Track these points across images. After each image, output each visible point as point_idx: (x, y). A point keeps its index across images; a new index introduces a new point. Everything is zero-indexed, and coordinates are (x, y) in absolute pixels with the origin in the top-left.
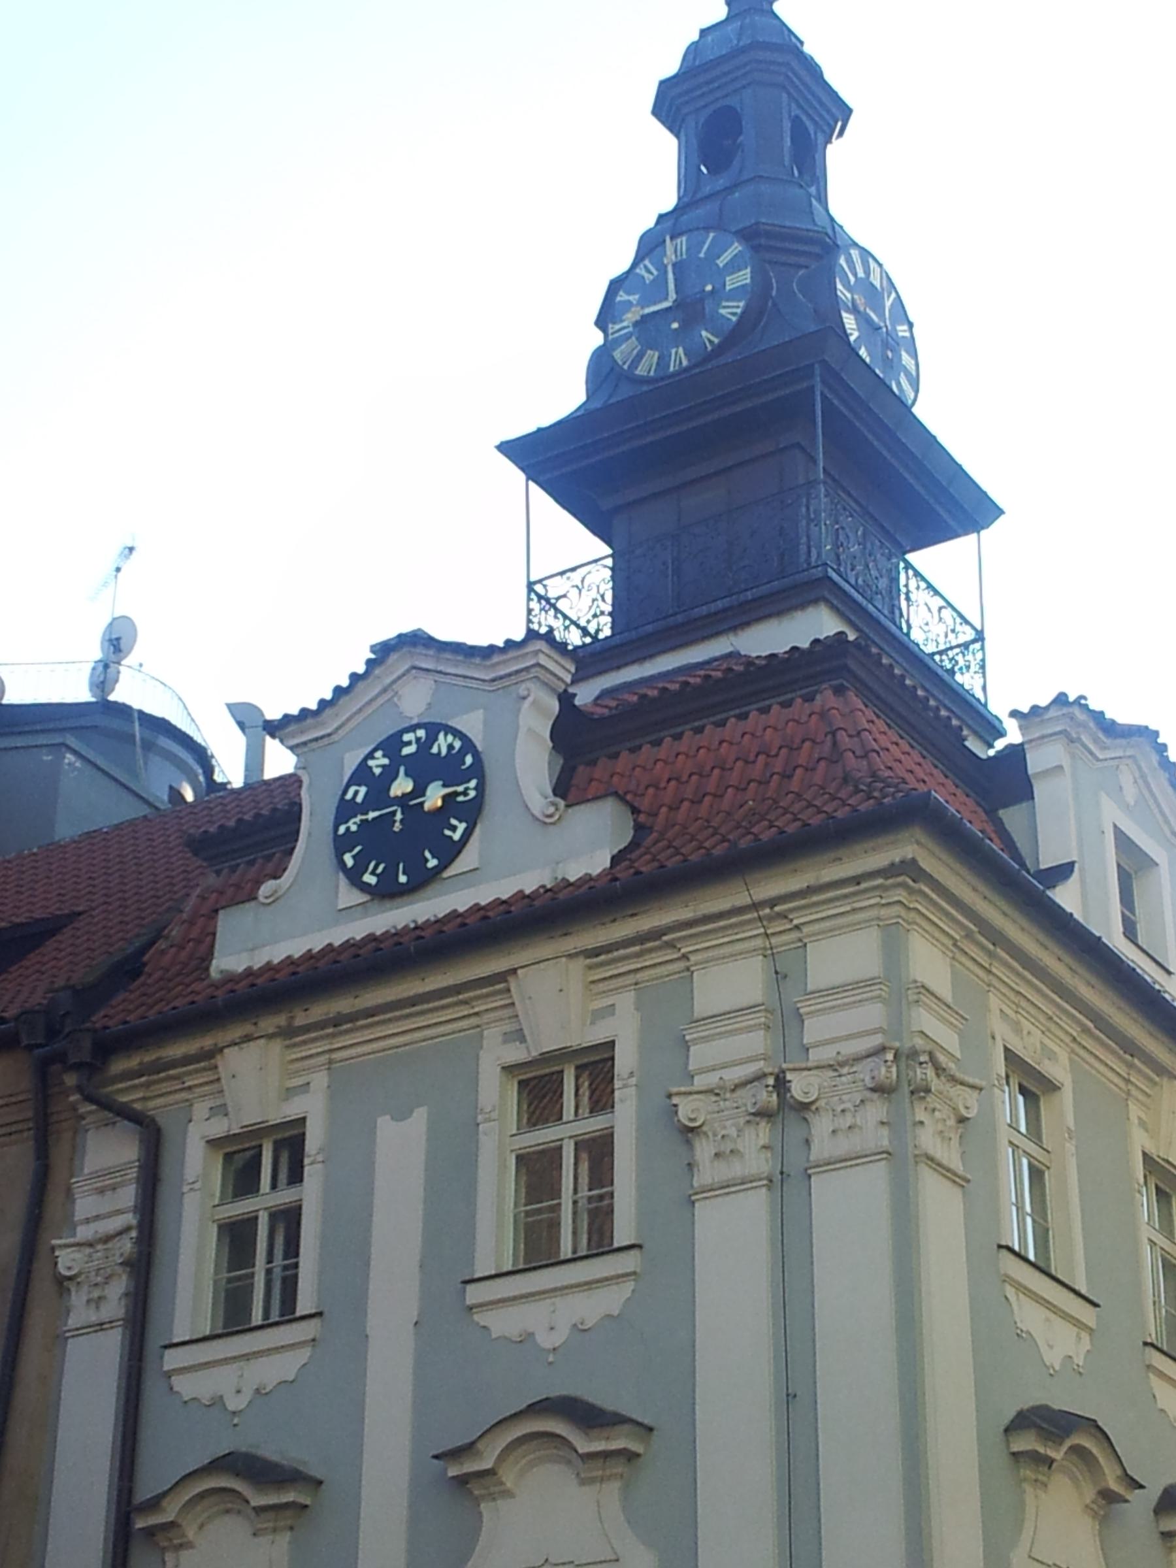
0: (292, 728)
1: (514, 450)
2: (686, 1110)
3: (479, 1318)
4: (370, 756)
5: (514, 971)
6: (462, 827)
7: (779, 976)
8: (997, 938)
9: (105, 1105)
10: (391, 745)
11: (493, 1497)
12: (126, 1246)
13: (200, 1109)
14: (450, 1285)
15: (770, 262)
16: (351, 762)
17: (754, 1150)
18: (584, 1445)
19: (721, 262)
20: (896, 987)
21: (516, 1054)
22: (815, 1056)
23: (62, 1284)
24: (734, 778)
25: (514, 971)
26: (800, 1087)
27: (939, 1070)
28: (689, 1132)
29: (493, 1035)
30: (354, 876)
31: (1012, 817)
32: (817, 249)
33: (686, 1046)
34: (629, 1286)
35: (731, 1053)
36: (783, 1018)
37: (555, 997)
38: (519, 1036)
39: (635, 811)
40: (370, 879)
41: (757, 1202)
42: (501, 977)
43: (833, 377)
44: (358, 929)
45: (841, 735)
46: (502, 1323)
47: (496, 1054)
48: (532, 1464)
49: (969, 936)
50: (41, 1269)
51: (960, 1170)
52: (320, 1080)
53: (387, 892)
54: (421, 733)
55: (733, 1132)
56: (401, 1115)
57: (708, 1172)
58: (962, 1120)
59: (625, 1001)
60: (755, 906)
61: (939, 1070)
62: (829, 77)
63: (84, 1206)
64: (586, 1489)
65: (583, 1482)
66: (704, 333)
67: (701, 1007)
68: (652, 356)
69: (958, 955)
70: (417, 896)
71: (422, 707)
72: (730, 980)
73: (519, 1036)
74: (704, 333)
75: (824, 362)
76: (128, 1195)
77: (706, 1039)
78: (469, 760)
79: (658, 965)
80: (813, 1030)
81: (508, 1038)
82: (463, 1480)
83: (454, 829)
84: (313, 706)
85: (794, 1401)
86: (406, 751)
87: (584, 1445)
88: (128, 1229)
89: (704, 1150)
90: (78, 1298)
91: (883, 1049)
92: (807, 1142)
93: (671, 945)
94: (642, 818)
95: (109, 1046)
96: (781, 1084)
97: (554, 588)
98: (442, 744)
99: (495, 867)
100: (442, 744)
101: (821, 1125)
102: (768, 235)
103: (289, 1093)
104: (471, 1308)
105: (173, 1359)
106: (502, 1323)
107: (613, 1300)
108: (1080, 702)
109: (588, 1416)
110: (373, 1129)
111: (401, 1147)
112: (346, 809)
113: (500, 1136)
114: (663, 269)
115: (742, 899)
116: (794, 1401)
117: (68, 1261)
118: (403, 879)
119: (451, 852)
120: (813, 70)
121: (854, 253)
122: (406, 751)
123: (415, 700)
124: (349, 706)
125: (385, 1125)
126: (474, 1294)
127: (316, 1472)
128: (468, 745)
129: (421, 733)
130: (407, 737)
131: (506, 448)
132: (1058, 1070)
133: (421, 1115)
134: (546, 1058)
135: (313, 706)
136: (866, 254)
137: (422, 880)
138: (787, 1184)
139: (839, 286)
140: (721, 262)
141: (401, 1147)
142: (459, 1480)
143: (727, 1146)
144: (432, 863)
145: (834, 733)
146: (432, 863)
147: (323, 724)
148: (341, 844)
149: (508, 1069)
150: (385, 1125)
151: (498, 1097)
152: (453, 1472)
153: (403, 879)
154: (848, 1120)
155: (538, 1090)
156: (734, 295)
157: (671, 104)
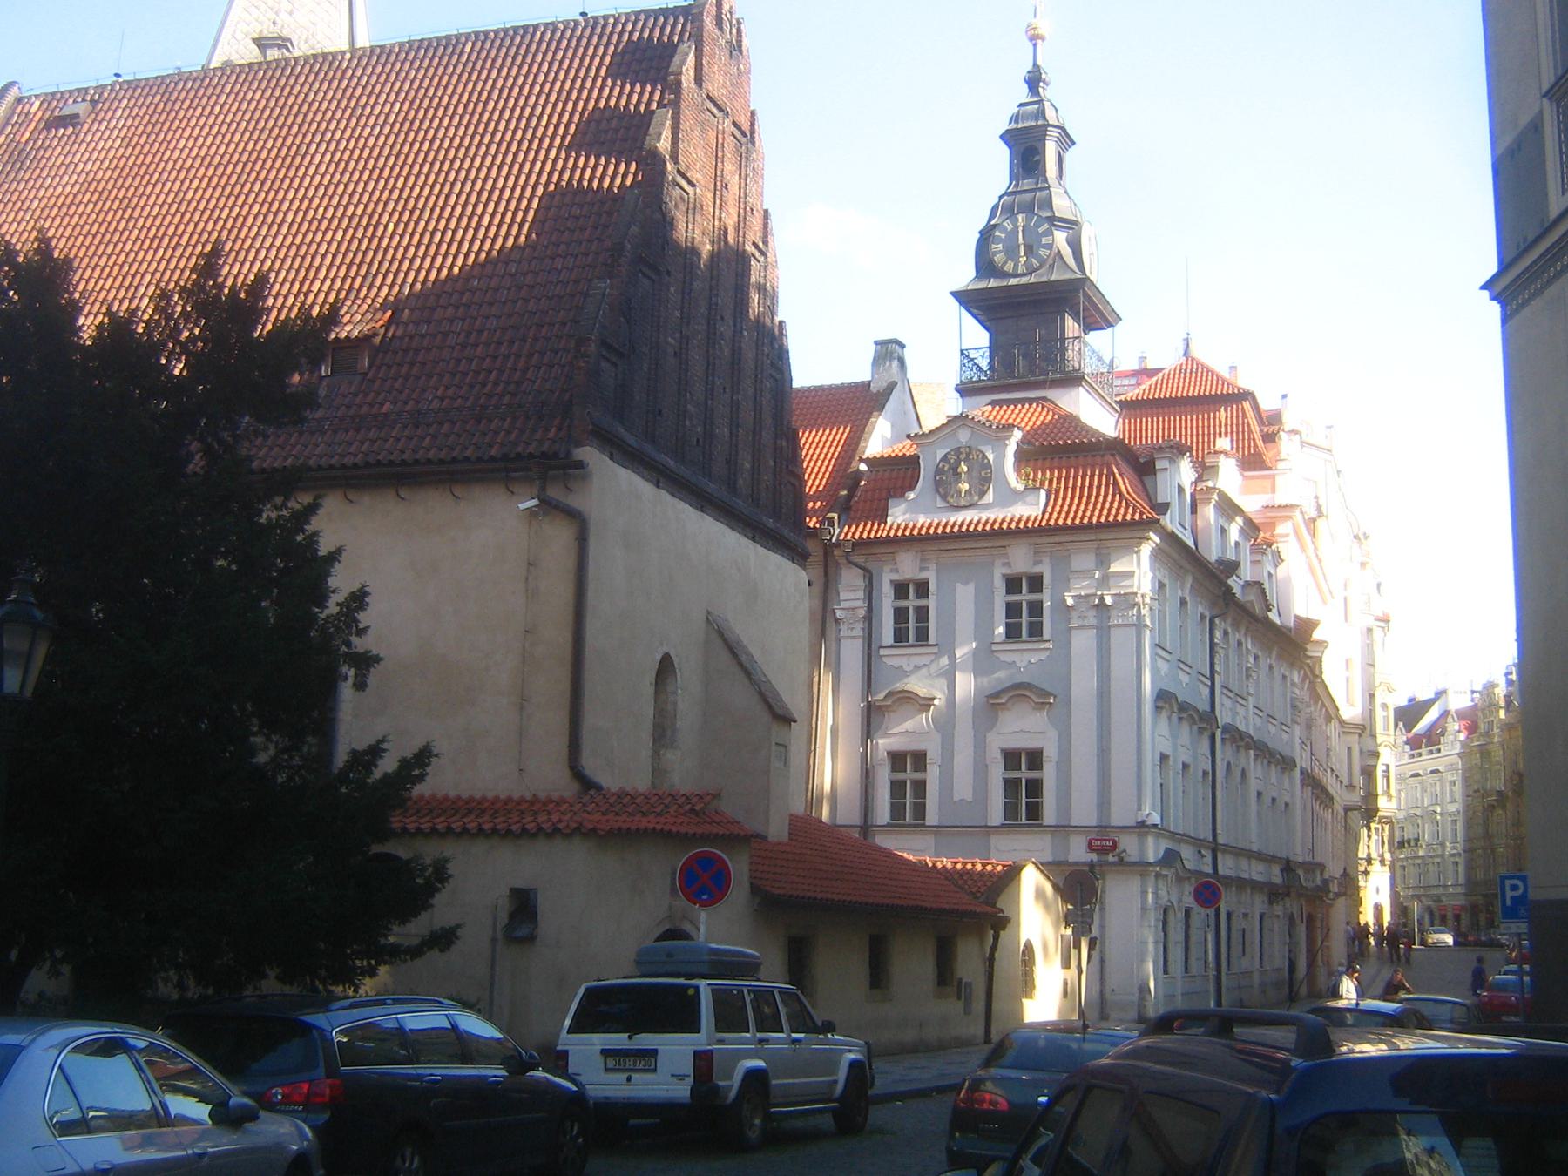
1: (955, 294)
12: (862, 612)
13: (887, 568)
16: (940, 454)
23: (837, 621)
29: (998, 562)
30: (944, 498)
31: (1147, 480)
38: (1008, 565)
43: (1086, 295)
46: (1004, 657)
50: (829, 615)
56: (966, 583)
63: (842, 596)
72: (1083, 560)
73: (1008, 565)
76: (861, 594)
81: (1004, 565)
90: (843, 627)
97: (973, 354)
103: (922, 569)
105: (882, 652)
106: (1004, 657)
111: (965, 595)
112: (938, 471)
113: (1000, 600)
114: (1016, 228)
117: (839, 614)
123: (964, 436)
125: (959, 585)
126: (994, 648)
131: (954, 294)
132: (1166, 581)
133: (971, 587)
141: (965, 595)
150: (960, 588)
157: (1007, 137)
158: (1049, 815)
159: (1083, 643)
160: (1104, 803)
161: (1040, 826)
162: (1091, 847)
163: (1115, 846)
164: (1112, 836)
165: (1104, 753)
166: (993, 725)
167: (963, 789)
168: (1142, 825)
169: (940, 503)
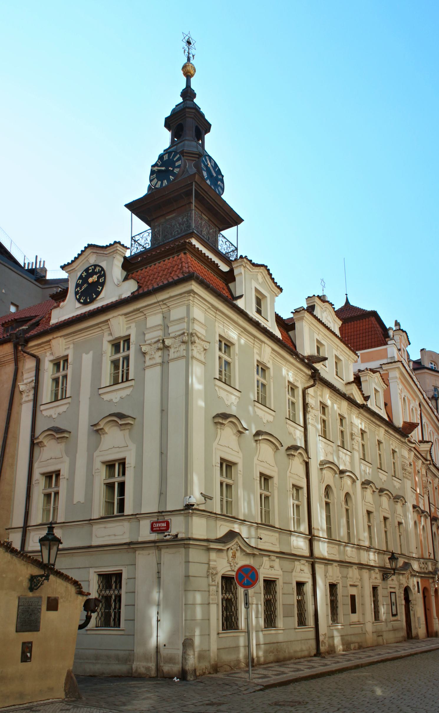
0: (66, 267)
2: (144, 349)
3: (102, 397)
4: (83, 273)
5: (109, 319)
6: (101, 288)
7: (164, 317)
8: (217, 309)
9: (28, 353)
10: (87, 270)
11: (103, 434)
14: (97, 390)
15: (187, 159)
17: (158, 357)
18: (120, 422)
19: (175, 159)
20: (189, 319)
21: (111, 338)
22: (171, 335)
24: (160, 275)
25: (109, 319)
26: (167, 342)
27: (198, 338)
28: (144, 354)
29: (106, 334)
30: (79, 300)
32: (197, 156)
33: (144, 334)
34: (131, 389)
35: (152, 336)
36: (166, 327)
37: (119, 324)
38: (111, 334)
39: (138, 283)
40: (82, 301)
41: (158, 369)
42: (107, 321)
44: (79, 312)
45: (184, 263)
46: (106, 397)
47: (107, 338)
48: (112, 427)
49: (209, 308)
51: (204, 361)
52: (71, 346)
53: (85, 303)
54: (93, 267)
55: (153, 353)
57: (148, 363)
58: (205, 350)
59: (133, 325)
60: (158, 302)
61: (198, 338)
62: (207, 117)
64: (122, 432)
65: (121, 430)
66: (171, 177)
67: (149, 325)
68: (159, 183)
69: (207, 313)
70: (92, 304)
71: (94, 261)
72: (154, 319)
74: (171, 177)
75: (195, 182)
77: (149, 333)
78: (103, 272)
79: (139, 316)
80: (171, 330)
82: (97, 431)
83: (99, 288)
84: (70, 262)
85: (164, 411)
86: (90, 271)
87: (120, 422)
88: (33, 381)
89: (147, 357)
91: (184, 333)
92: (169, 355)
93: (142, 312)
94: (141, 285)
95: (27, 341)
96: (163, 342)
98: (97, 269)
99: (107, 296)
100: (97, 269)
101: (172, 350)
102: (186, 153)
104: (100, 394)
106: (106, 397)
107: (128, 391)
108: (246, 257)
109: (121, 416)
110: (81, 357)
112: (77, 285)
115: (155, 300)
116: (164, 411)
118: (88, 300)
119: (98, 294)
120: (202, 116)
121: (207, 158)
122: (90, 271)
124: (78, 262)
126: (101, 391)
127: (69, 430)
128: (103, 269)
129: (93, 267)
130: (90, 268)
134: (117, 339)
135: (70, 262)
136: (210, 158)
137: (92, 300)
138: (164, 364)
139: (202, 165)
140: (175, 159)
142: (97, 431)
143: (151, 357)
144: (95, 296)
145: (182, 263)
146: (95, 296)
147: (72, 266)
148: (76, 293)
149: (109, 342)
150: (84, 356)
151: (108, 348)
152: (95, 429)
153: (88, 300)
154: (177, 349)
155: (116, 347)
156: (177, 167)
158: (128, 510)
159: (152, 376)
160: (162, 494)
161: (123, 516)
162: (153, 530)
163: (168, 523)
164: (166, 518)
165: (163, 454)
166: (97, 447)
167: (79, 496)
168: (189, 506)
169: (78, 305)
